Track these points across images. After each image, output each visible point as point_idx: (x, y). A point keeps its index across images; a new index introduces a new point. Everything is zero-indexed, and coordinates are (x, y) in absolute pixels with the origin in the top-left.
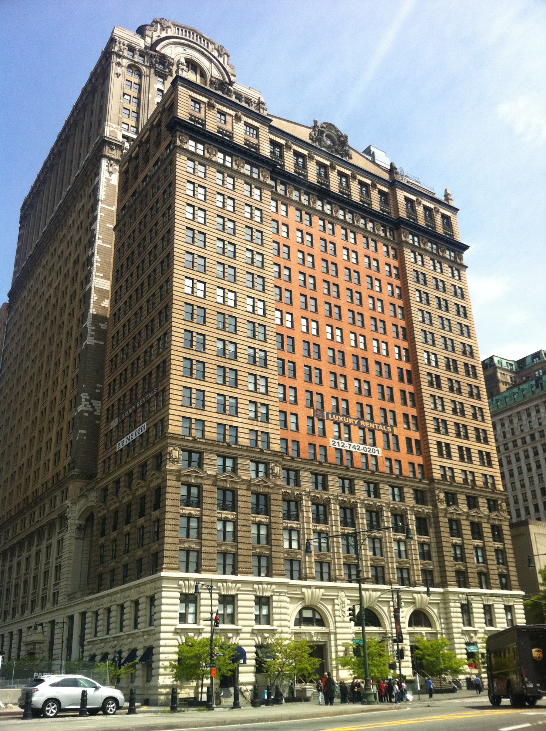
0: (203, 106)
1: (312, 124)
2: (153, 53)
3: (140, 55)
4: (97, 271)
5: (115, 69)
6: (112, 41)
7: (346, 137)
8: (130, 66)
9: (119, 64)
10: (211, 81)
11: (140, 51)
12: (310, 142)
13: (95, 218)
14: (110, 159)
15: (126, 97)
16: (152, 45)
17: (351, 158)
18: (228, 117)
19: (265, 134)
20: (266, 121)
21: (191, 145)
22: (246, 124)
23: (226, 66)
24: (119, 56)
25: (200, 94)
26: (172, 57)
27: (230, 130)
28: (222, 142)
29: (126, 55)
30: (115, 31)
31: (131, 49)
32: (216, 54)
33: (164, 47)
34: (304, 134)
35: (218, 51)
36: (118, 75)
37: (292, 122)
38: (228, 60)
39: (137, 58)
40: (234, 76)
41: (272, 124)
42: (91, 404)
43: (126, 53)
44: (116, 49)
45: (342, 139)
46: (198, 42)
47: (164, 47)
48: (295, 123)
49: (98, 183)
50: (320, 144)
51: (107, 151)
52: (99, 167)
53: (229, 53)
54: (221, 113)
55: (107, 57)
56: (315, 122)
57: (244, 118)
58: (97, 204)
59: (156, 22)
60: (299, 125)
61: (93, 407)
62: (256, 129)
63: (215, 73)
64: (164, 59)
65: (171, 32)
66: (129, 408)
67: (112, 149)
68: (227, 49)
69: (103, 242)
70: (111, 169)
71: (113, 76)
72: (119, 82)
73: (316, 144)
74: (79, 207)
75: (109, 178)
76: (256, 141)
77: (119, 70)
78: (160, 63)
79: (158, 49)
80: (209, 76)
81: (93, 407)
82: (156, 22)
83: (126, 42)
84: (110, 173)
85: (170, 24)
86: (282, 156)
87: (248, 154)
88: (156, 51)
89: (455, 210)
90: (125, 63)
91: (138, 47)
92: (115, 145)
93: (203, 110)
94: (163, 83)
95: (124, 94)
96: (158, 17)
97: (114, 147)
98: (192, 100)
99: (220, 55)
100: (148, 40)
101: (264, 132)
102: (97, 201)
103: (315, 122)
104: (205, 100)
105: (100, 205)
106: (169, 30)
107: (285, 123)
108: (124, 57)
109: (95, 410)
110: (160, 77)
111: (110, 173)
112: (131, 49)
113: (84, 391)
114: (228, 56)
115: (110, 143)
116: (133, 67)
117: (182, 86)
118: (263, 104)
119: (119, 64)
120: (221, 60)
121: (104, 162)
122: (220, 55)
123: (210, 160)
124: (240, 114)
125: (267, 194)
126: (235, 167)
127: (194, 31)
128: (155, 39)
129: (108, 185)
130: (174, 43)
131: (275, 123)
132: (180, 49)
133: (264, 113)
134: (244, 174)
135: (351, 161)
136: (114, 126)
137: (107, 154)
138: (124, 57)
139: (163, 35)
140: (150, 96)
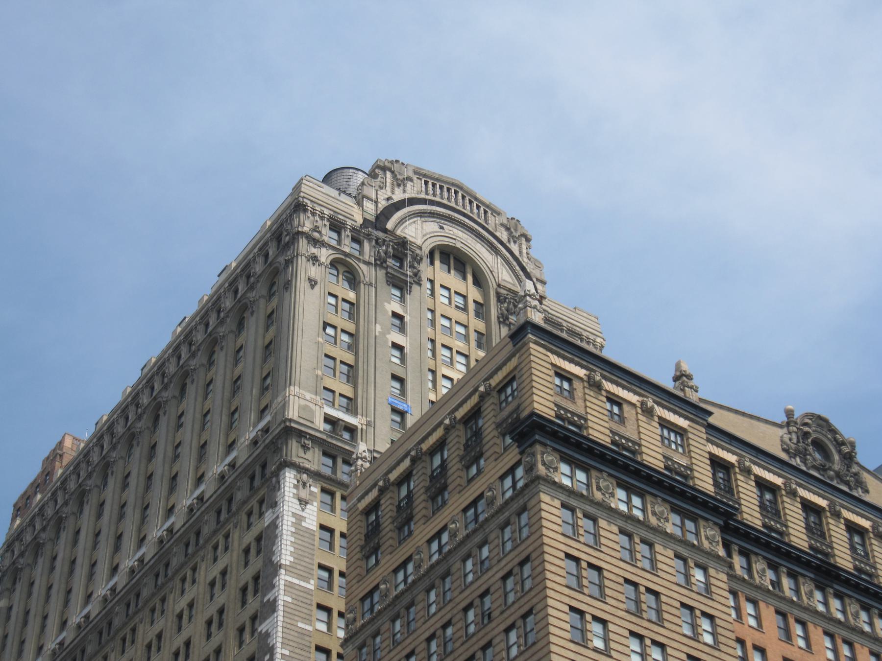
0: (577, 384)
1: (782, 418)
2: (381, 235)
3: (354, 240)
5: (305, 270)
6: (297, 206)
7: (853, 445)
8: (334, 264)
9: (314, 259)
10: (498, 295)
11: (353, 230)
12: (784, 456)
13: (271, 607)
14: (300, 469)
15: (330, 331)
16: (377, 218)
17: (867, 491)
18: (626, 407)
19: (702, 448)
20: (698, 412)
21: (563, 474)
22: (664, 424)
23: (524, 261)
24: (315, 242)
25: (571, 361)
26: (419, 242)
27: (635, 437)
28: (619, 464)
29: (326, 239)
30: (304, 188)
31: (336, 226)
32: (503, 235)
33: (402, 221)
34: (772, 440)
35: (508, 229)
36: (313, 283)
37: (743, 414)
38: (529, 247)
39: (348, 246)
40: (543, 283)
41: (711, 420)
43: (328, 236)
44: (307, 227)
45: (845, 449)
46: (467, 212)
47: (402, 221)
48: (751, 417)
49: (274, 526)
50: (804, 461)
51: (294, 451)
52: (276, 487)
53: (530, 233)
54: (614, 400)
55: (280, 240)
56: (789, 413)
57: (659, 411)
58: (275, 574)
59: (384, 169)
60: (759, 419)
62: (681, 432)
63: (505, 276)
64: (402, 249)
65: (414, 189)
67: (305, 448)
68: (527, 226)
70: (304, 494)
71: (301, 284)
72: (313, 299)
73: (797, 462)
74: (208, 572)
75: (300, 514)
76: (684, 461)
77: (314, 271)
78: (395, 257)
79: (390, 225)
80: (492, 285)
82: (384, 169)
83: (326, 212)
84: (303, 502)
85: (411, 174)
86: (729, 490)
87: (668, 487)
88: (385, 231)
90: (325, 255)
91: (349, 222)
92: (313, 439)
93: (579, 393)
94: (402, 299)
95: (326, 325)
96: (386, 155)
97: (309, 443)
98: (557, 374)
99: (511, 236)
100: (369, 206)
101: (698, 438)
102: (274, 568)
103: (789, 413)
104: (581, 372)
105: (283, 577)
106: (409, 185)
107: (732, 416)
108: (323, 244)
110: (395, 286)
111: (303, 502)
112: (336, 226)
114: (528, 240)
115: (301, 434)
116: (344, 267)
117: (536, 343)
118: (689, 377)
119: (314, 259)
120: (515, 248)
121: (289, 477)
122: (513, 238)
123: (603, 506)
124: (650, 403)
125: (720, 579)
126: (653, 521)
127: (459, 187)
128: (383, 204)
129: (299, 530)
130: (421, 214)
131: (718, 419)
132: (432, 226)
133: (693, 397)
134: (671, 537)
135: (867, 498)
136: (308, 396)
137: (295, 459)
138: (323, 244)
139: (399, 195)
140: (378, 328)
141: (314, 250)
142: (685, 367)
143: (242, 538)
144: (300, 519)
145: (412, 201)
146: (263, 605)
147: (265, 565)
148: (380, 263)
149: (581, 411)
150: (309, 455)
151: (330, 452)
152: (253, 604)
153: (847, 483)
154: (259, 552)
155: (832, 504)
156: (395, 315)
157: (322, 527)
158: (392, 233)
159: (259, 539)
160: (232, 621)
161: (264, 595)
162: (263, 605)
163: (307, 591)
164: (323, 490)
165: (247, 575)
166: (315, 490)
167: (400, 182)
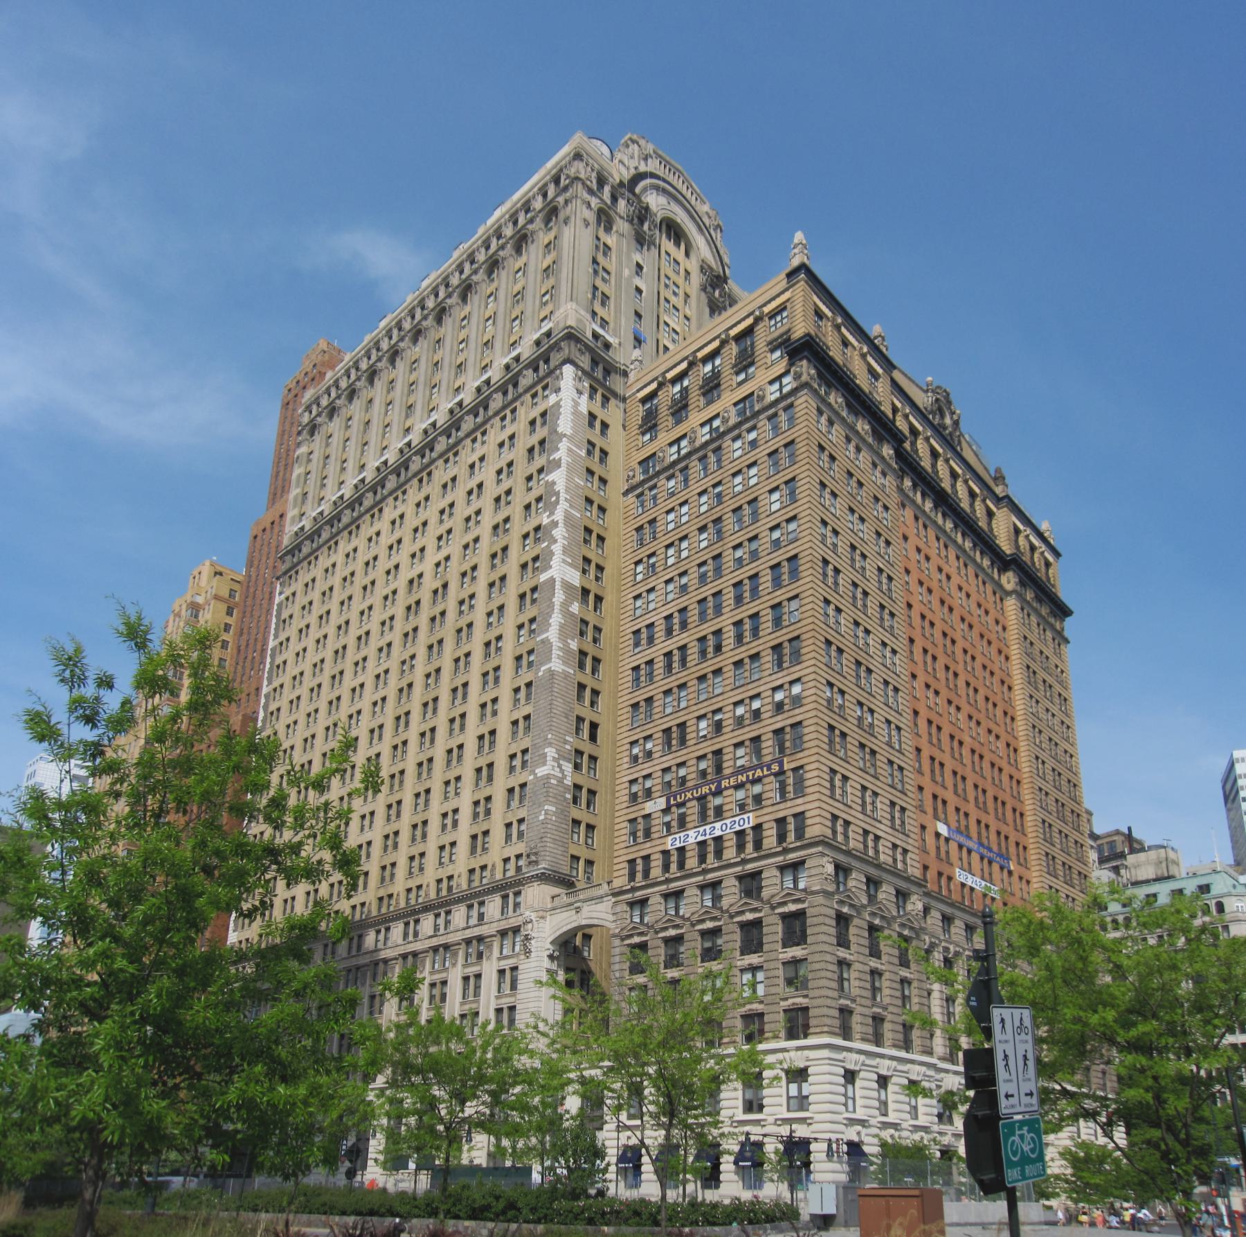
4: (565, 551)
33: (645, 190)
42: (560, 766)
47: (645, 190)
49: (558, 405)
61: (562, 771)
64: (642, 214)
66: (696, 787)
79: (637, 190)
81: (562, 771)
84: (580, 392)
88: (634, 194)
109: (564, 777)
113: (550, 745)
128: (633, 171)
130: (657, 188)
139: (643, 168)
143: (526, 412)
144: (576, 404)
145: (653, 175)
146: (549, 462)
147: (550, 433)
150: (582, 358)
152: (539, 461)
154: (544, 423)
156: (638, 265)
157: (590, 414)
158: (638, 197)
159: (544, 414)
160: (521, 470)
161: (549, 455)
162: (549, 462)
163: (580, 456)
164: (591, 386)
165: (534, 440)
166: (586, 385)
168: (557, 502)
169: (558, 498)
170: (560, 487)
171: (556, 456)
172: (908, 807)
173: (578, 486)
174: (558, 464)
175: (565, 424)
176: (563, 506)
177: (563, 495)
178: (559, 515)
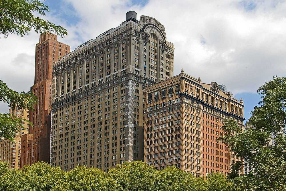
12: (210, 90)
49: (128, 89)
54: (192, 87)
67: (133, 76)
69: (132, 111)
79: (144, 31)
84: (133, 85)
88: (144, 32)
89: (243, 106)
100: (141, 26)
115: (132, 74)
121: (130, 81)
124: (196, 87)
128: (143, 26)
129: (132, 90)
141: (133, 38)
142: (201, 79)
144: (132, 88)
148: (143, 39)
149: (188, 90)
151: (136, 76)
153: (217, 92)
155: (215, 96)
167: (146, 21)
168: (129, 111)
169: (129, 110)
170: (130, 107)
171: (128, 100)
172: (200, 152)
173: (133, 106)
174: (129, 102)
175: (130, 94)
176: (130, 111)
177: (130, 109)
178: (129, 113)
